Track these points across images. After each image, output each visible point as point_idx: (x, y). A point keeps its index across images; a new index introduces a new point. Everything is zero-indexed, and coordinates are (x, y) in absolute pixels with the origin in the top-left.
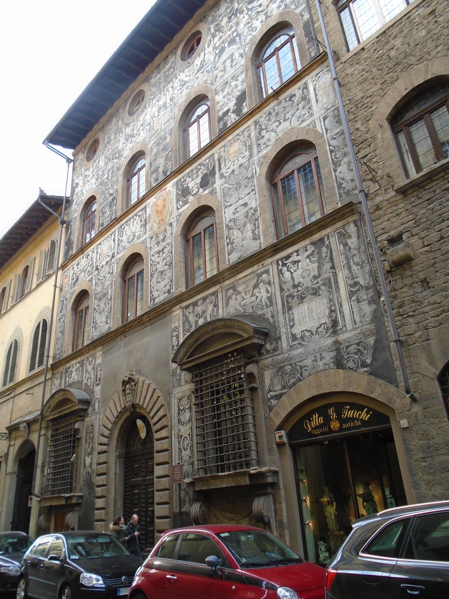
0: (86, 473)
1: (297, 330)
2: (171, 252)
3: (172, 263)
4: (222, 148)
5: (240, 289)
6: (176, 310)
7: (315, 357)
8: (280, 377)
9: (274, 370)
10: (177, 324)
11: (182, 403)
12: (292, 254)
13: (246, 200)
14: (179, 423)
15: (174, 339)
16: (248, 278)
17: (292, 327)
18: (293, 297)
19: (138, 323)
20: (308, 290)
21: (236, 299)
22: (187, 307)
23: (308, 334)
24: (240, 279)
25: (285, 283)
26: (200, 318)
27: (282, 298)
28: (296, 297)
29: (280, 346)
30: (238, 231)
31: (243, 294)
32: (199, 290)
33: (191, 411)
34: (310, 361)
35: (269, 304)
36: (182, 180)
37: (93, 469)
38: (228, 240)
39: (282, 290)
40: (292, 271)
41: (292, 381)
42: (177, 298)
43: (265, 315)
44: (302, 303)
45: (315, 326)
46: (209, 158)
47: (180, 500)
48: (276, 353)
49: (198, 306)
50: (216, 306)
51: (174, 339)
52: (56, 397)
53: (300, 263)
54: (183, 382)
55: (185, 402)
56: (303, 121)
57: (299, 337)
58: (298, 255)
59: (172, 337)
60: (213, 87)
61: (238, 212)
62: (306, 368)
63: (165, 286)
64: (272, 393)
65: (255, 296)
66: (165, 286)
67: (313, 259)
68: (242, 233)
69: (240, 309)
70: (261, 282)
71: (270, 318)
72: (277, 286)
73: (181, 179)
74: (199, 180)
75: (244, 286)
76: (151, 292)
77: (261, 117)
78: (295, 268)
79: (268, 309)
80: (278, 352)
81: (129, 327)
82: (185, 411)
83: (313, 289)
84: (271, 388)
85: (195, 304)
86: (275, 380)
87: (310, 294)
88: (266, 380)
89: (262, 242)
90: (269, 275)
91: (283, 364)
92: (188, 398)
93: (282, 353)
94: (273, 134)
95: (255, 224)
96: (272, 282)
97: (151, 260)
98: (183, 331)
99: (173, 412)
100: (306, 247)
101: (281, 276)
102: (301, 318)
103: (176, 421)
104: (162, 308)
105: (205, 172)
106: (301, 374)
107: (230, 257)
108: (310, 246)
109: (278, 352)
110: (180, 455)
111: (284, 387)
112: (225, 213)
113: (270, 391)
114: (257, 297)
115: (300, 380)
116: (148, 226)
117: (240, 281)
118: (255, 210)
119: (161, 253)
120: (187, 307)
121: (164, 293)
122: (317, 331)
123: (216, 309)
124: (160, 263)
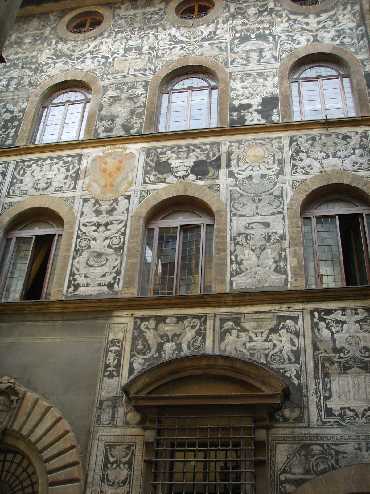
1: (335, 404)
2: (124, 234)
3: (122, 248)
4: (235, 142)
5: (247, 325)
6: (122, 317)
7: (359, 444)
8: (303, 457)
9: (295, 446)
10: (120, 336)
11: (115, 452)
12: (336, 310)
13: (269, 219)
14: (103, 481)
15: (111, 356)
16: (262, 316)
17: (326, 398)
18: (333, 363)
19: (38, 309)
20: (355, 361)
21: (238, 337)
22: (144, 319)
23: (349, 413)
24: (248, 313)
25: (321, 341)
26: (168, 341)
27: (315, 359)
28: (336, 364)
29: (306, 418)
30: (251, 252)
31: (253, 335)
32: (173, 304)
33: (130, 468)
34: (352, 448)
35: (293, 359)
36: (159, 150)
38: (233, 257)
39: (315, 348)
40: (334, 330)
41: (322, 467)
42: (129, 301)
43: (286, 371)
44: (344, 373)
45: (362, 407)
46: (212, 144)
48: (298, 425)
49: (165, 323)
50: (201, 333)
51: (111, 356)
53: (345, 325)
54: (119, 421)
55: (118, 452)
56: (359, 169)
57: (337, 413)
58: (343, 315)
59: (108, 352)
60: (228, 70)
61: (252, 228)
62: (345, 455)
63: (104, 275)
64: (288, 476)
65: (271, 343)
66: (104, 275)
67: (365, 327)
68: (258, 257)
69: (244, 351)
70: (283, 327)
71: (293, 377)
72: (309, 341)
73: (158, 148)
74: (190, 162)
75: (254, 324)
76: (72, 274)
77: (301, 137)
78: (337, 329)
79: (292, 365)
80: (302, 425)
82: (118, 465)
83: (362, 362)
84: (288, 469)
85: (161, 320)
86: (295, 459)
87: (357, 367)
88: (279, 457)
89: (289, 279)
90: (297, 324)
91: (309, 442)
92: (127, 448)
93: (309, 427)
94: (316, 164)
95: (280, 255)
96: (301, 333)
97: (79, 229)
98: (132, 350)
99: (93, 462)
100: (356, 310)
101: (316, 330)
102: (342, 390)
103: (98, 477)
104: (97, 304)
105: (202, 157)
106: (337, 461)
107: (233, 279)
108: (362, 310)
109: (302, 425)
111: (307, 472)
112: (231, 221)
113: (284, 471)
114: (274, 345)
115: (334, 468)
116: (80, 182)
117: (248, 316)
118: (282, 237)
119: (101, 229)
120: (144, 319)
121: (99, 285)
122: (363, 414)
123: (200, 339)
124: (98, 241)
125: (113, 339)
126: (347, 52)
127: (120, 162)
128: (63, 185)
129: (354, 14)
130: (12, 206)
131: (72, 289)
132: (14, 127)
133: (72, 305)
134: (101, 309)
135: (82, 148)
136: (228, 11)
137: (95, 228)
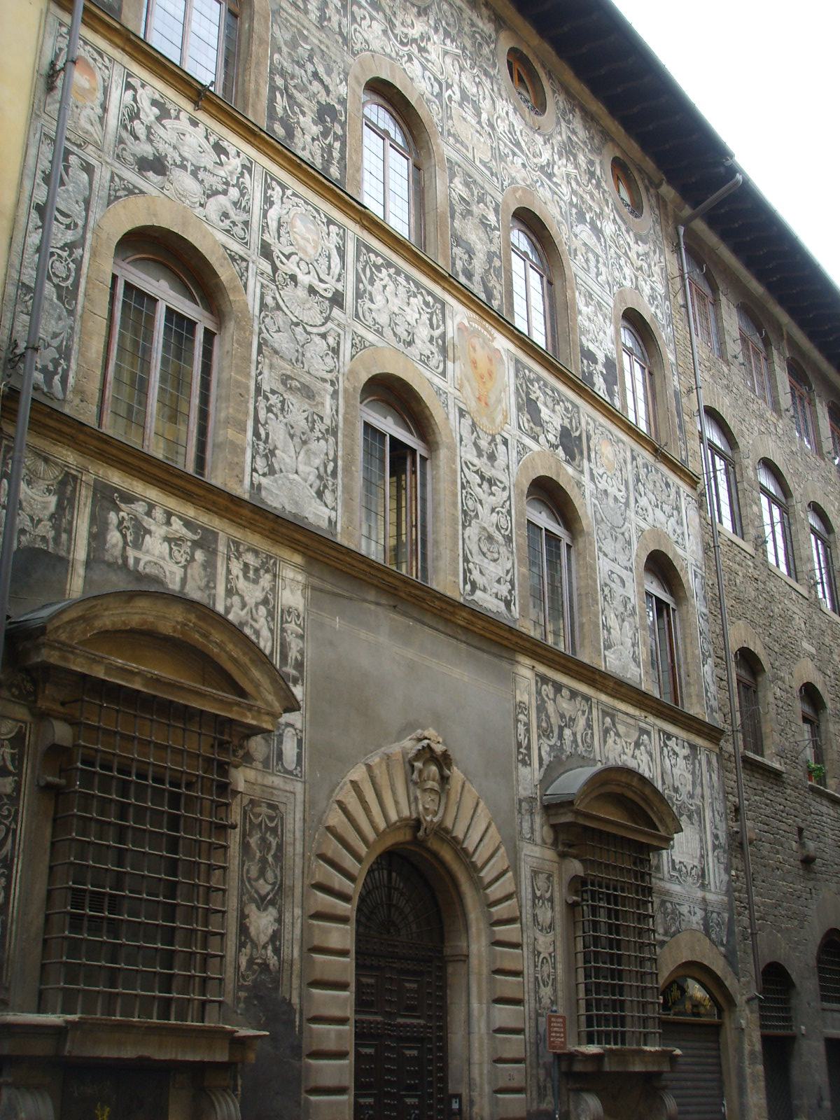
0: (251, 961)
19: (442, 610)
32: (570, 669)
37: (285, 951)
47: (539, 1088)
51: (521, 728)
52: (142, 604)
76: (466, 560)
81: (416, 597)
110: (536, 992)
125: (521, 702)
126: (661, 336)
127: (490, 360)
128: (429, 353)
129: (662, 269)
130: (365, 347)
131: (468, 587)
132: (336, 138)
133: (480, 622)
134: (505, 642)
135: (444, 288)
136: (560, 133)
137: (478, 480)
